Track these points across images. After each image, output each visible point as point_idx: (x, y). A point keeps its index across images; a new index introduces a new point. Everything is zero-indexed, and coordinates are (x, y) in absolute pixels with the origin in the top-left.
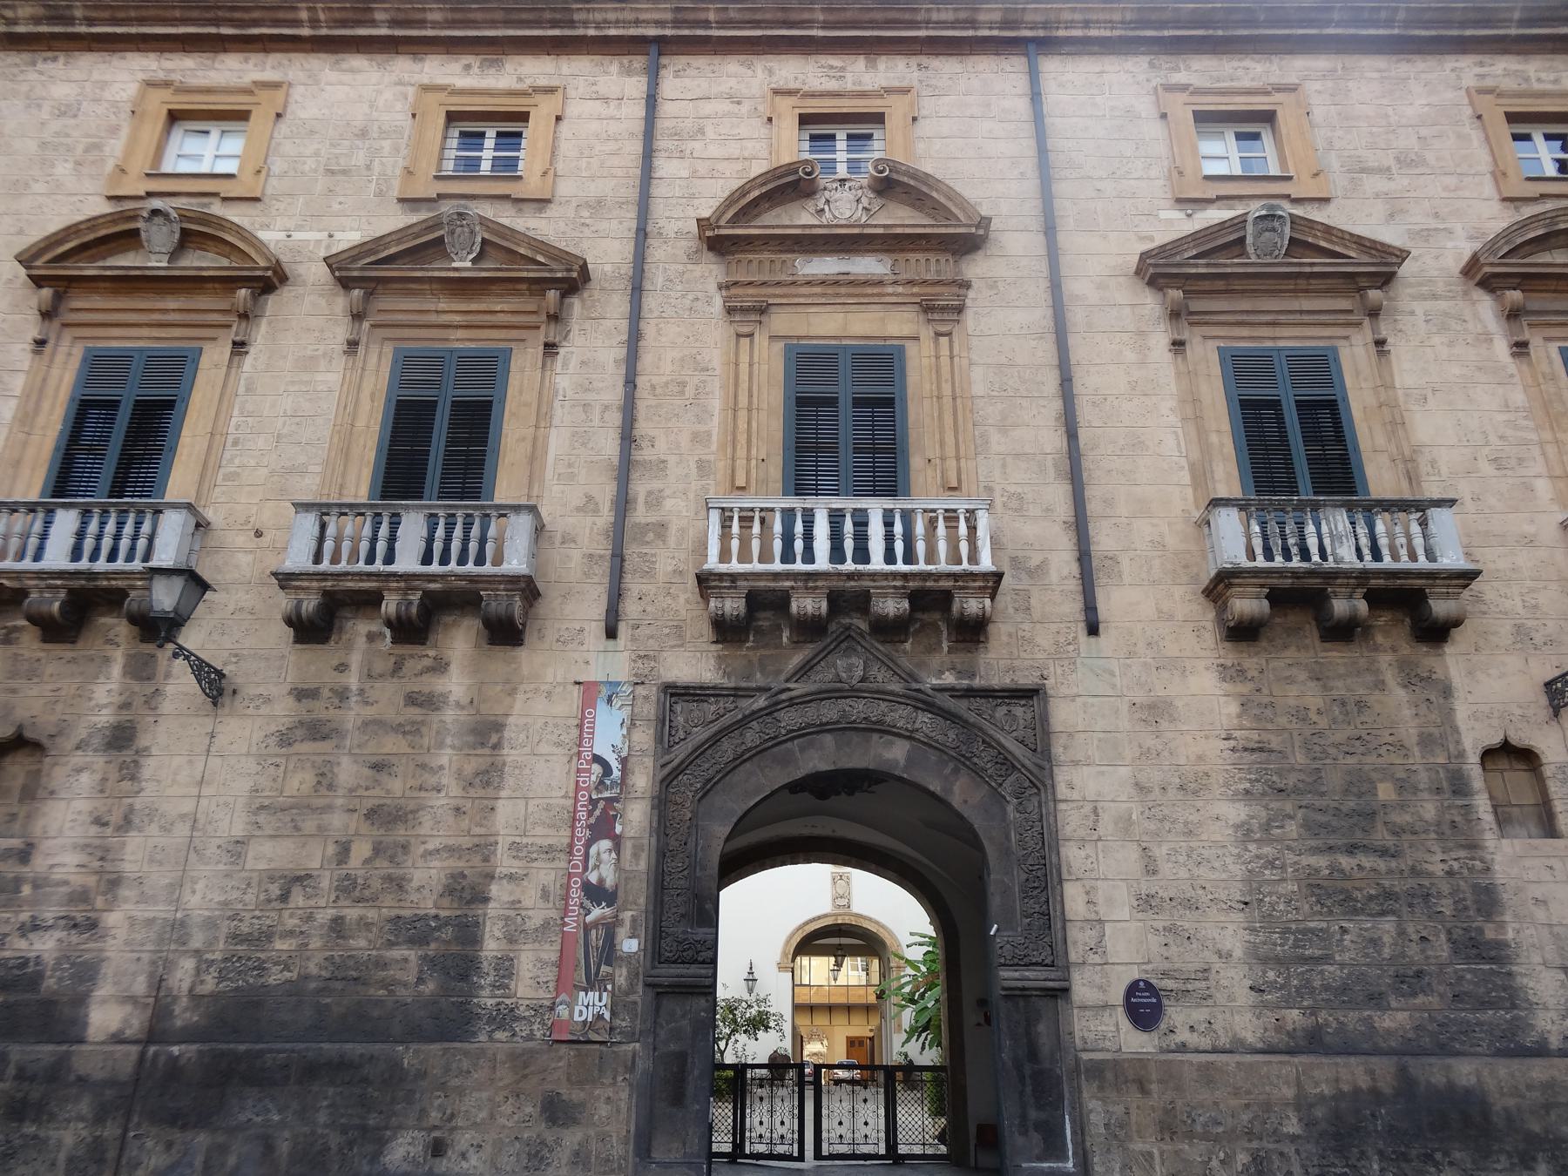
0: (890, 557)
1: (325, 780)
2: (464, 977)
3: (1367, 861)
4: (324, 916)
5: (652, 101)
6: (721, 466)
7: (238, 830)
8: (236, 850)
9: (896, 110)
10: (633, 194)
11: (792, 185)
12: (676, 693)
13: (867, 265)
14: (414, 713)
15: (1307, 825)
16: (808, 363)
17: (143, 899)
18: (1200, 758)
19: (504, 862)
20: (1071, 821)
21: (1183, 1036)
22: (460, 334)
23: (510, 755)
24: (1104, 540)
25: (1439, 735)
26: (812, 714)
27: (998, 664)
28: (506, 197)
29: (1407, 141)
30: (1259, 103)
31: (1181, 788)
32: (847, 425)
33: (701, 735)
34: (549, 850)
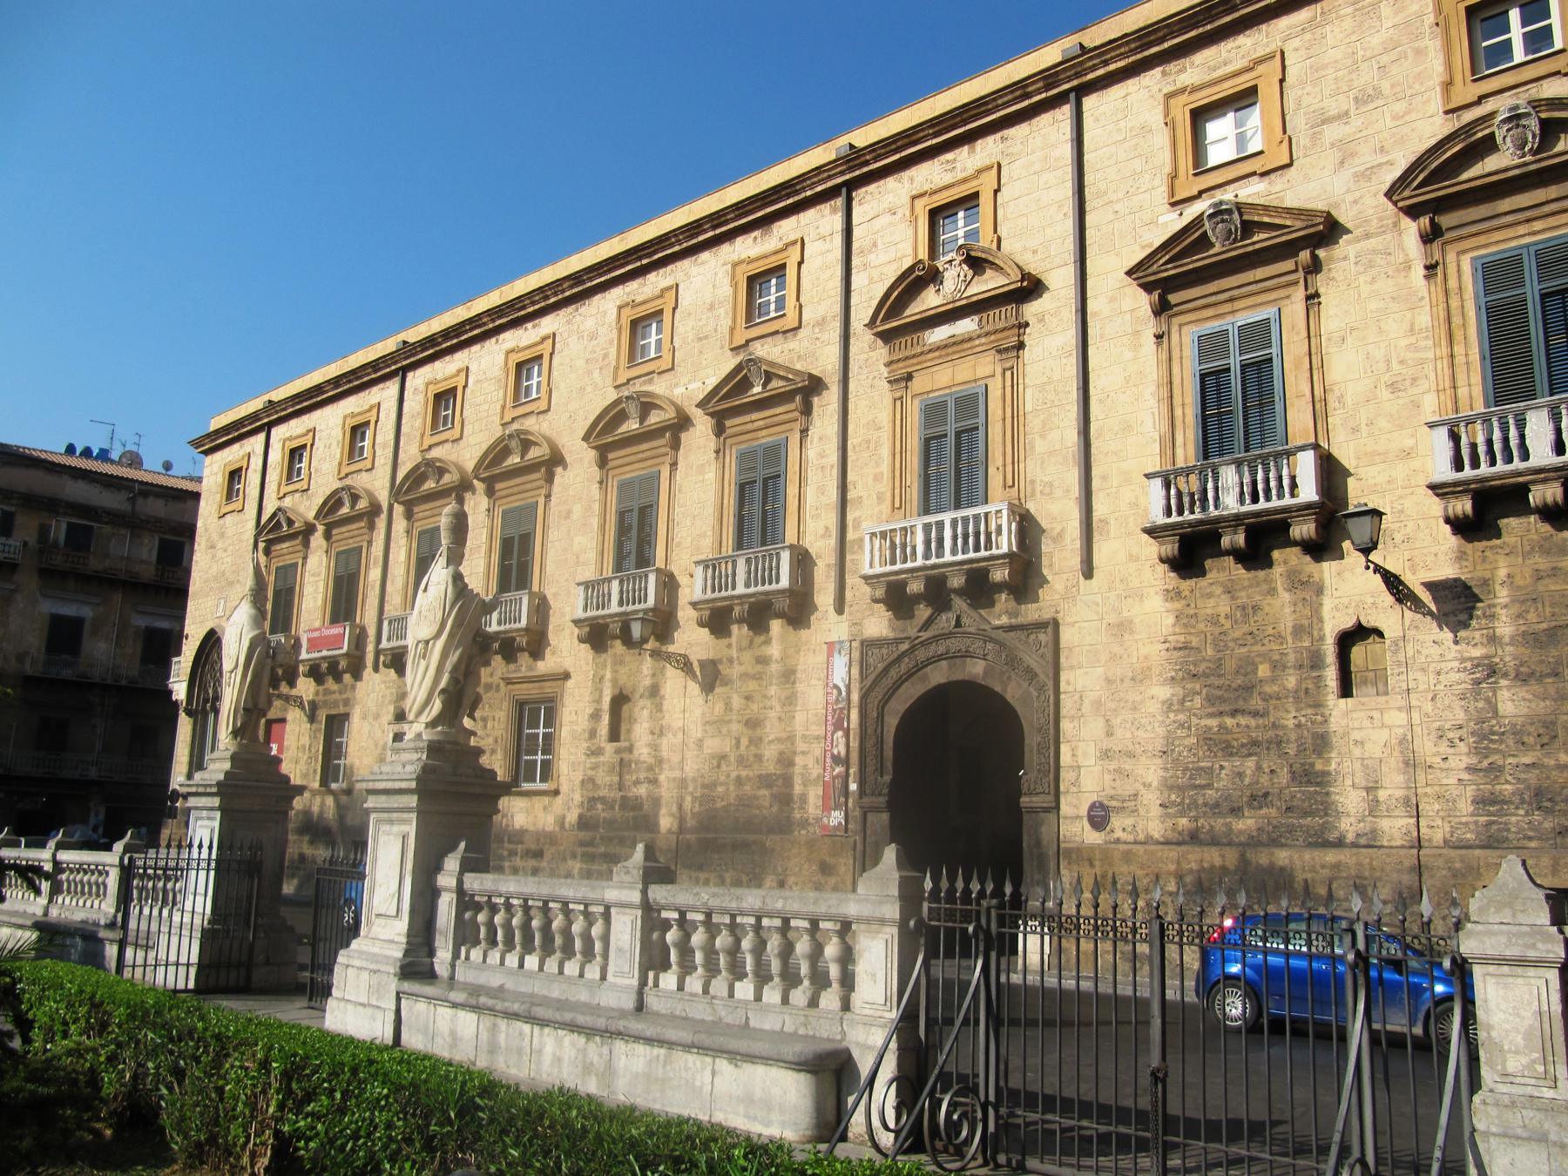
0: (954, 552)
1: (728, 707)
2: (788, 804)
3: (1243, 720)
4: (734, 775)
6: (889, 494)
7: (699, 735)
8: (700, 743)
9: (986, 185)
10: (837, 308)
11: (917, 279)
12: (868, 645)
14: (759, 668)
15: (1210, 700)
16: (933, 412)
17: (672, 769)
18: (1146, 657)
19: (801, 746)
21: (1119, 834)
22: (764, 432)
23: (800, 687)
25: (1307, 628)
26: (933, 650)
28: (777, 332)
29: (1366, 77)
30: (1242, 83)
31: (1133, 679)
32: (952, 454)
33: (881, 666)
34: (817, 738)
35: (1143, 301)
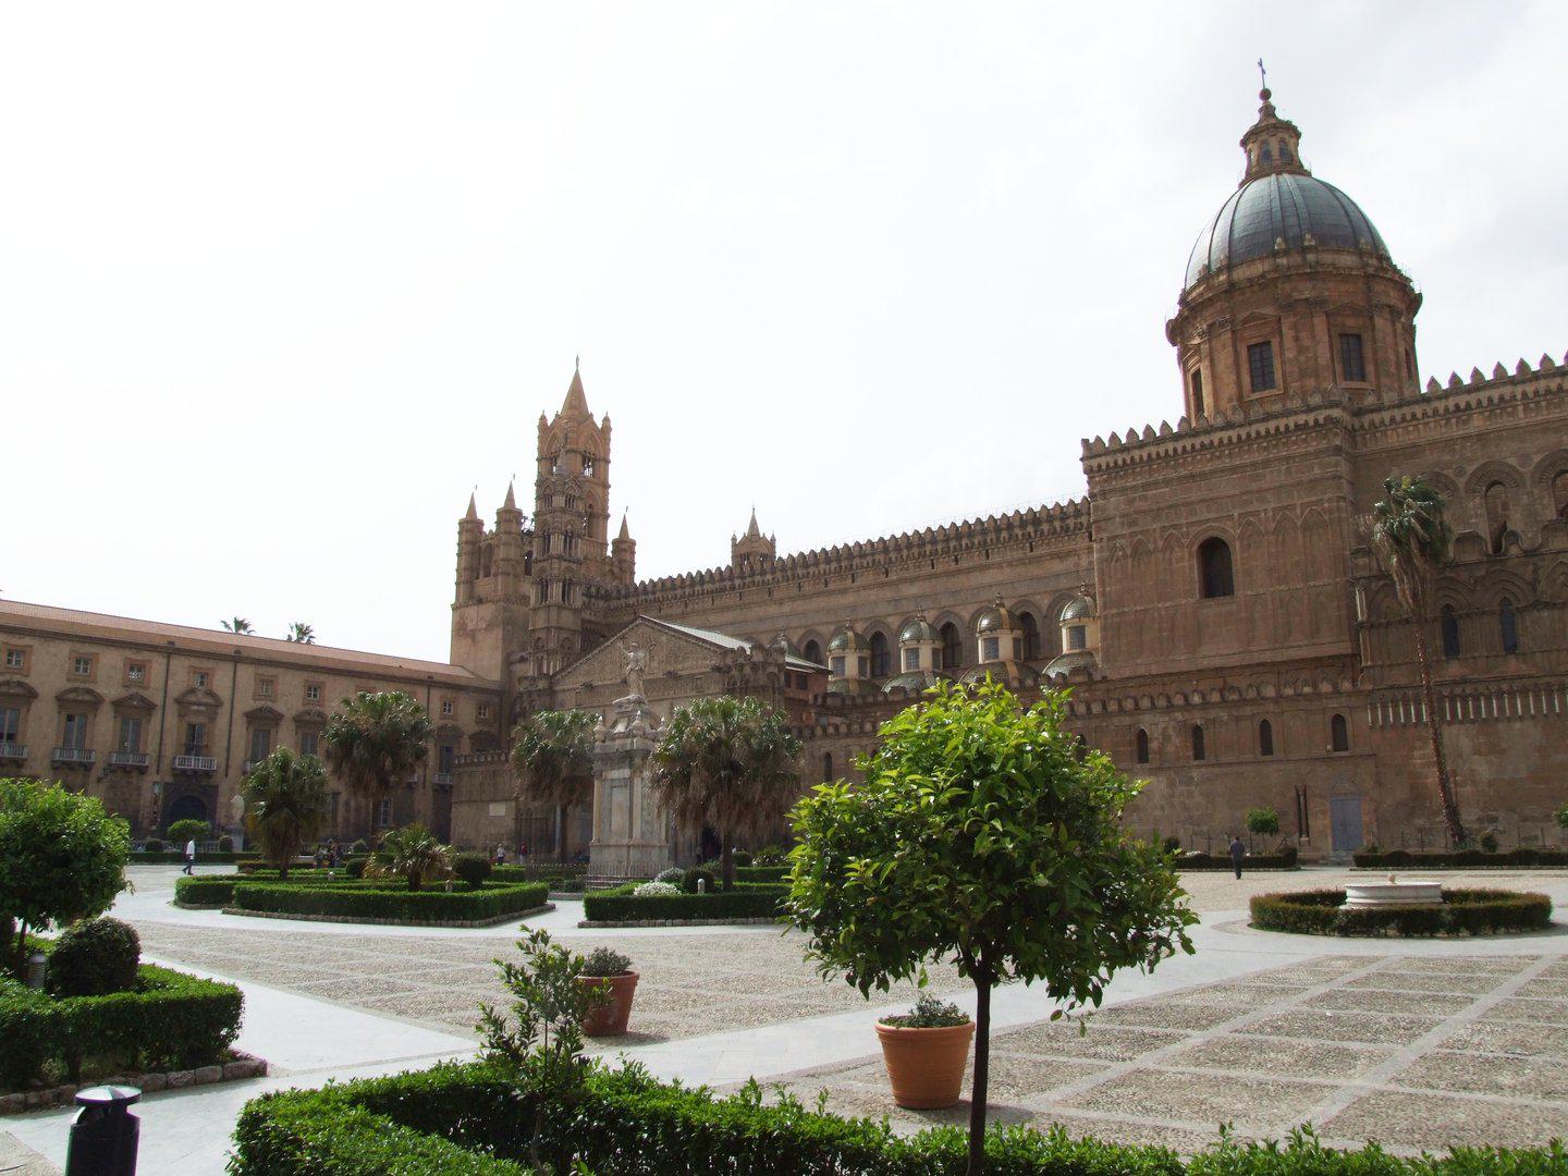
1: (116, 795)
5: (168, 665)
11: (193, 691)
12: (167, 784)
13: (203, 708)
32: (194, 741)
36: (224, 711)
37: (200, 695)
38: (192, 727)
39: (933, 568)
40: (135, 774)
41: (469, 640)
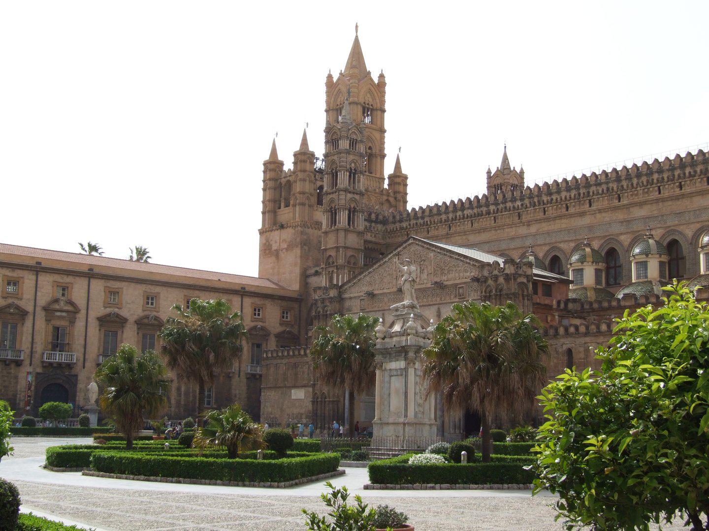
11: (56, 301)
12: (38, 374)
13: (64, 314)
20: (78, 389)
24: (87, 357)
27: (73, 372)
30: (117, 290)
35: (97, 323)
36: (82, 315)
37: (62, 303)
38: (57, 329)
39: (660, 193)
40: (13, 366)
41: (274, 259)
